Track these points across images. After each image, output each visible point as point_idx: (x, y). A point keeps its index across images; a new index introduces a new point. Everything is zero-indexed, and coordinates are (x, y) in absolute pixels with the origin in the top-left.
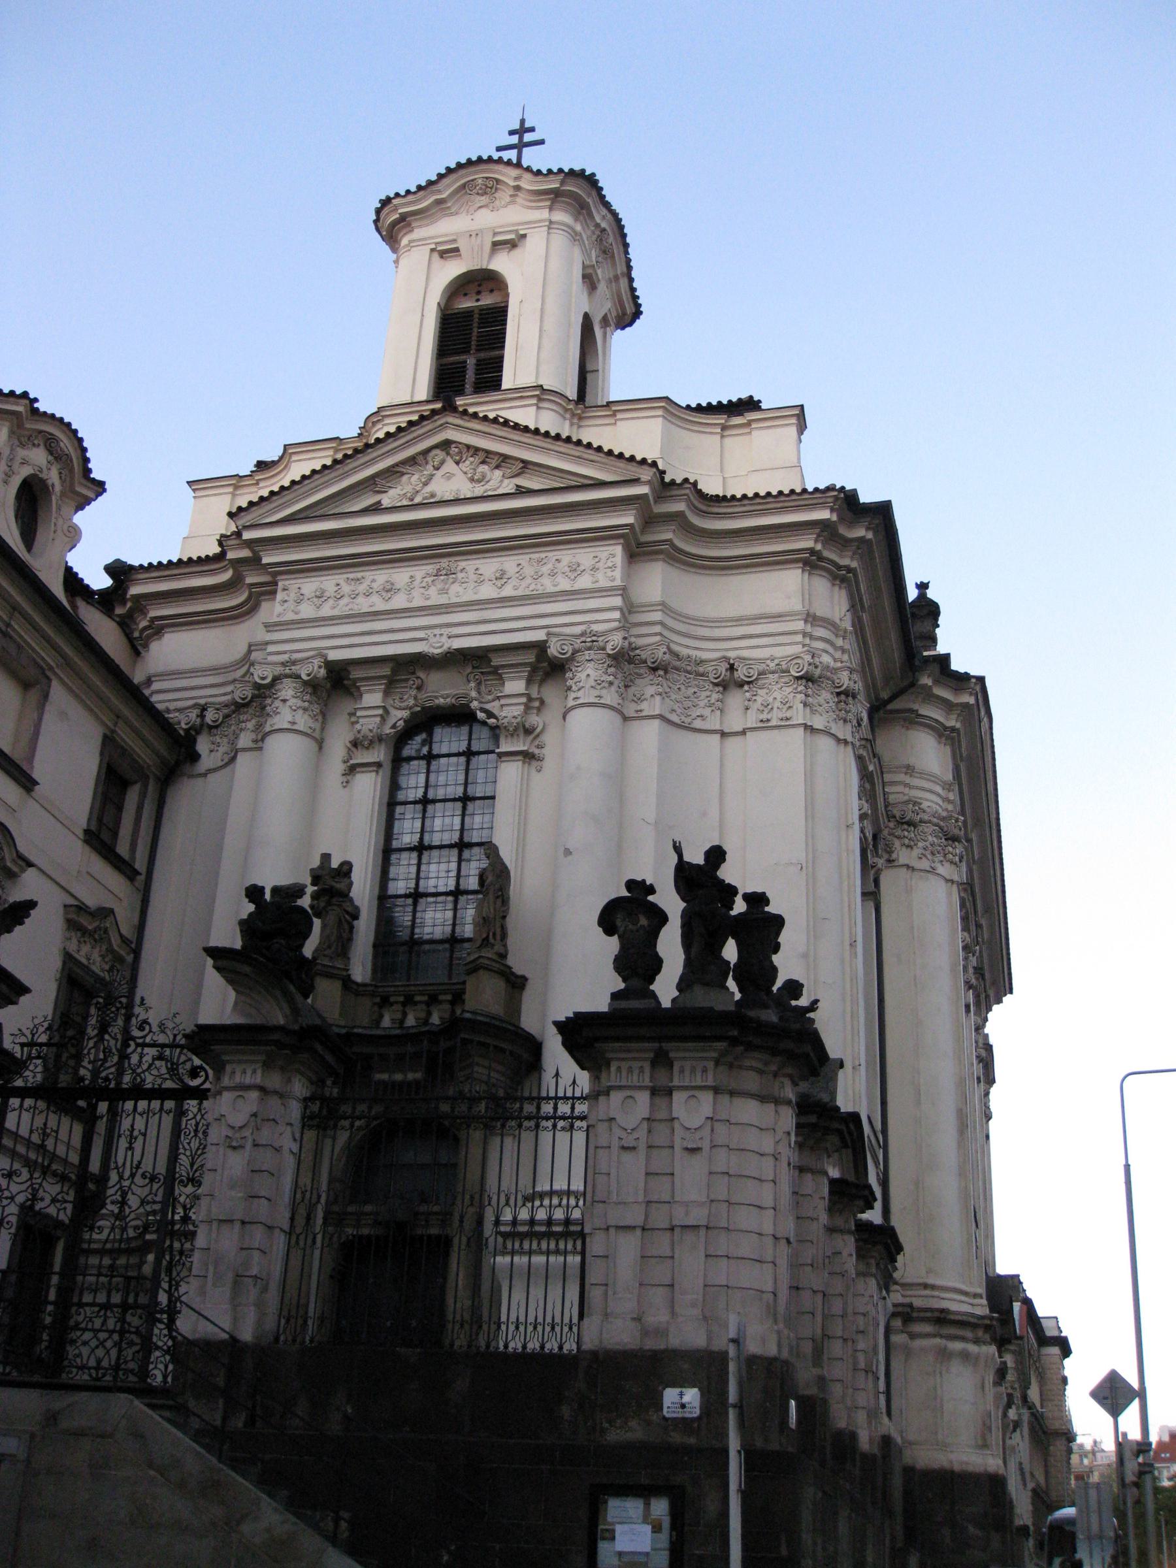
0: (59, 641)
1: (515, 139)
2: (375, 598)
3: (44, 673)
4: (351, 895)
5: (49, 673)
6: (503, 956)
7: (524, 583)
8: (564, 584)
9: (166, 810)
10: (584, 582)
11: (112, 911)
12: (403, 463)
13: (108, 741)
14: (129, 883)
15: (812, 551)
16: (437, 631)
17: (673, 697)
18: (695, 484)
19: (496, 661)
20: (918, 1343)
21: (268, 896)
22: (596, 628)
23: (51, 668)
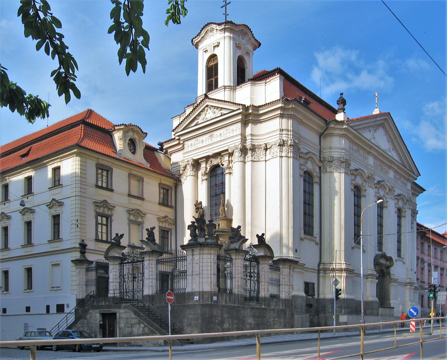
5: (143, 177)
16: (211, 150)
23: (143, 176)
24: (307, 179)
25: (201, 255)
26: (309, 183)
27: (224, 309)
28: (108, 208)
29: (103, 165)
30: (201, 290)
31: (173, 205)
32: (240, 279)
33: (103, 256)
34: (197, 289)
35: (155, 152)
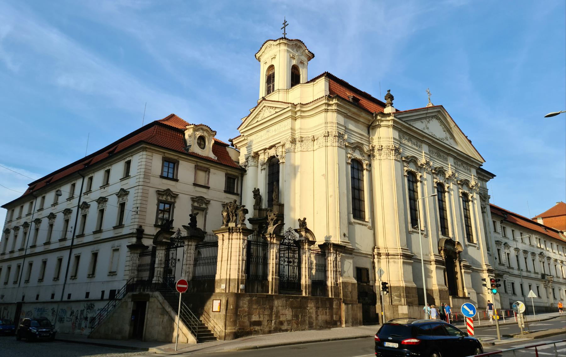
0: (209, 164)
1: (283, 26)
4: (260, 194)
8: (284, 129)
10: (286, 128)
12: (260, 112)
13: (227, 175)
14: (237, 196)
15: (325, 109)
18: (301, 103)
19: (277, 146)
22: (287, 137)
24: (356, 166)
25: (230, 240)
26: (358, 170)
29: (169, 158)
33: (152, 240)
35: (227, 148)
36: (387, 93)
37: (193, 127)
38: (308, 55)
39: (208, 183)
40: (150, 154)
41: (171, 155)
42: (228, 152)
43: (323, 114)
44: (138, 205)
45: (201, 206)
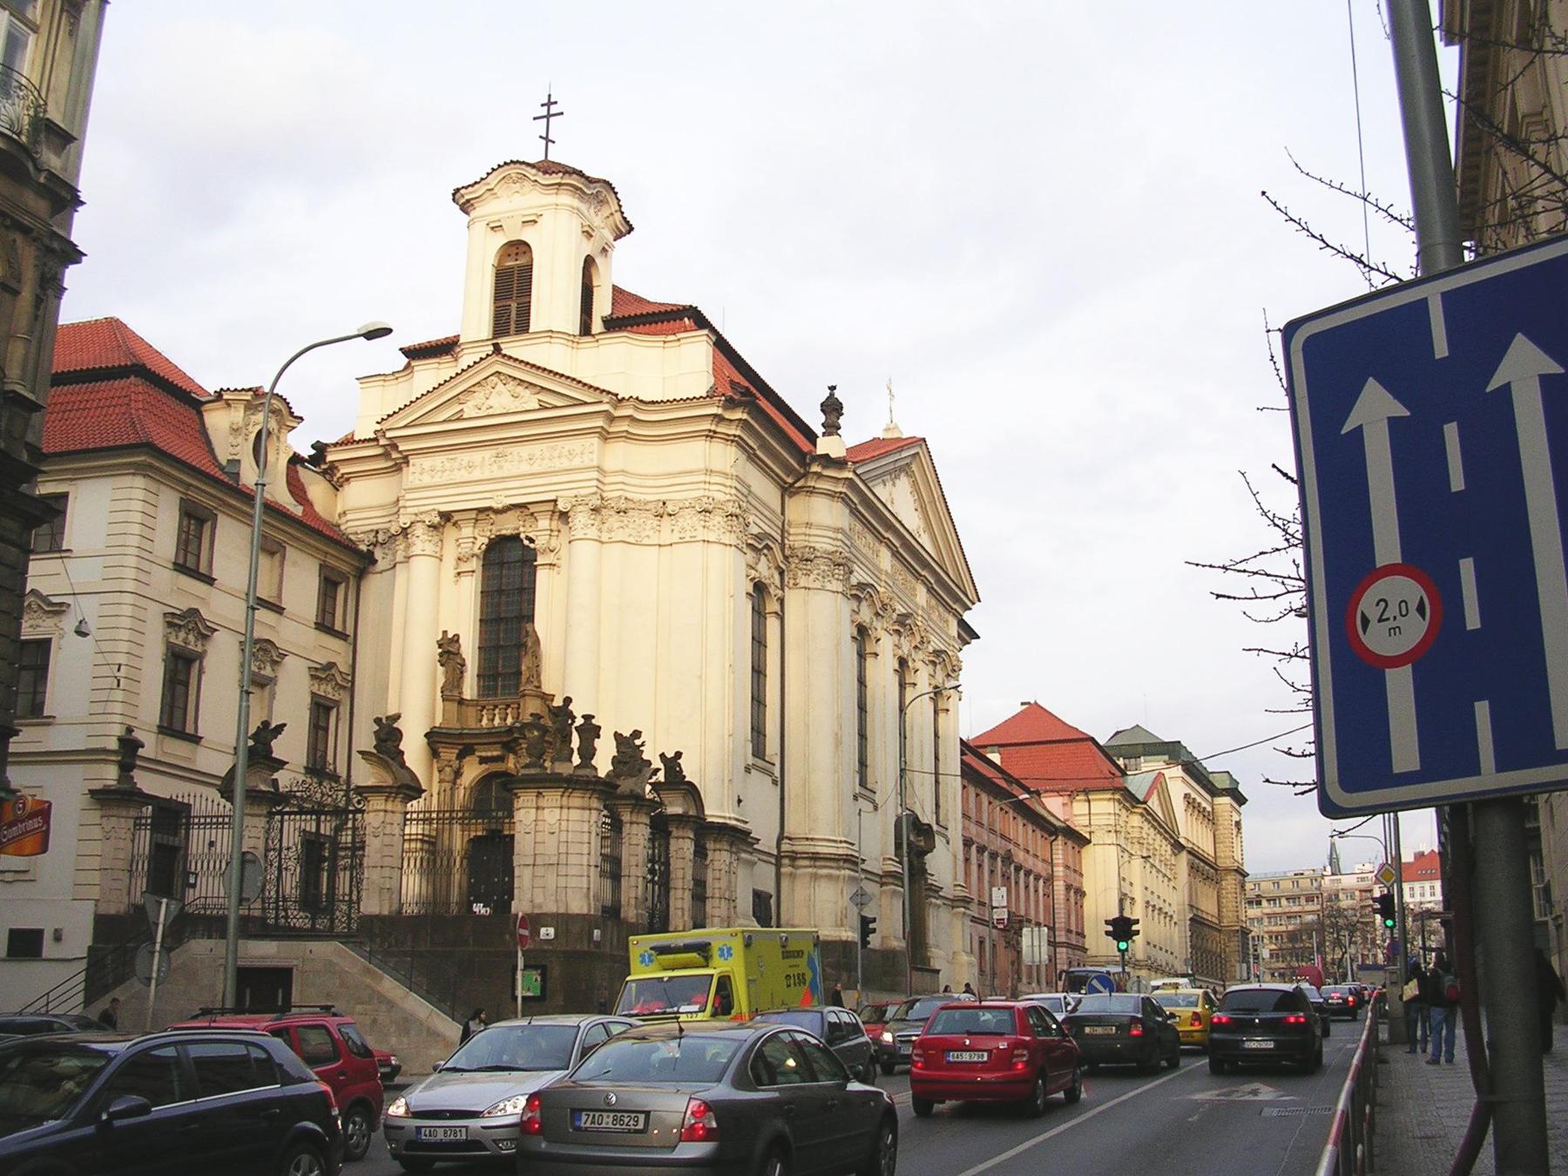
0: (286, 529)
1: (544, 111)
2: (463, 472)
3: (281, 544)
6: (539, 687)
7: (545, 462)
8: (566, 464)
9: (361, 593)
10: (576, 463)
11: (335, 664)
12: (474, 385)
14: (343, 642)
15: (710, 431)
16: (499, 493)
17: (631, 526)
18: (637, 398)
19: (533, 509)
20: (799, 871)
21: (384, 721)
22: (583, 492)
27: (616, 965)
28: (200, 633)
30: (562, 910)
31: (350, 631)
32: (640, 879)
34: (550, 908)
36: (828, 393)
37: (249, 398)
38: (618, 228)
39: (279, 596)
40: (153, 486)
41: (205, 496)
42: (302, 485)
43: (700, 445)
44: (122, 659)
45: (262, 672)
